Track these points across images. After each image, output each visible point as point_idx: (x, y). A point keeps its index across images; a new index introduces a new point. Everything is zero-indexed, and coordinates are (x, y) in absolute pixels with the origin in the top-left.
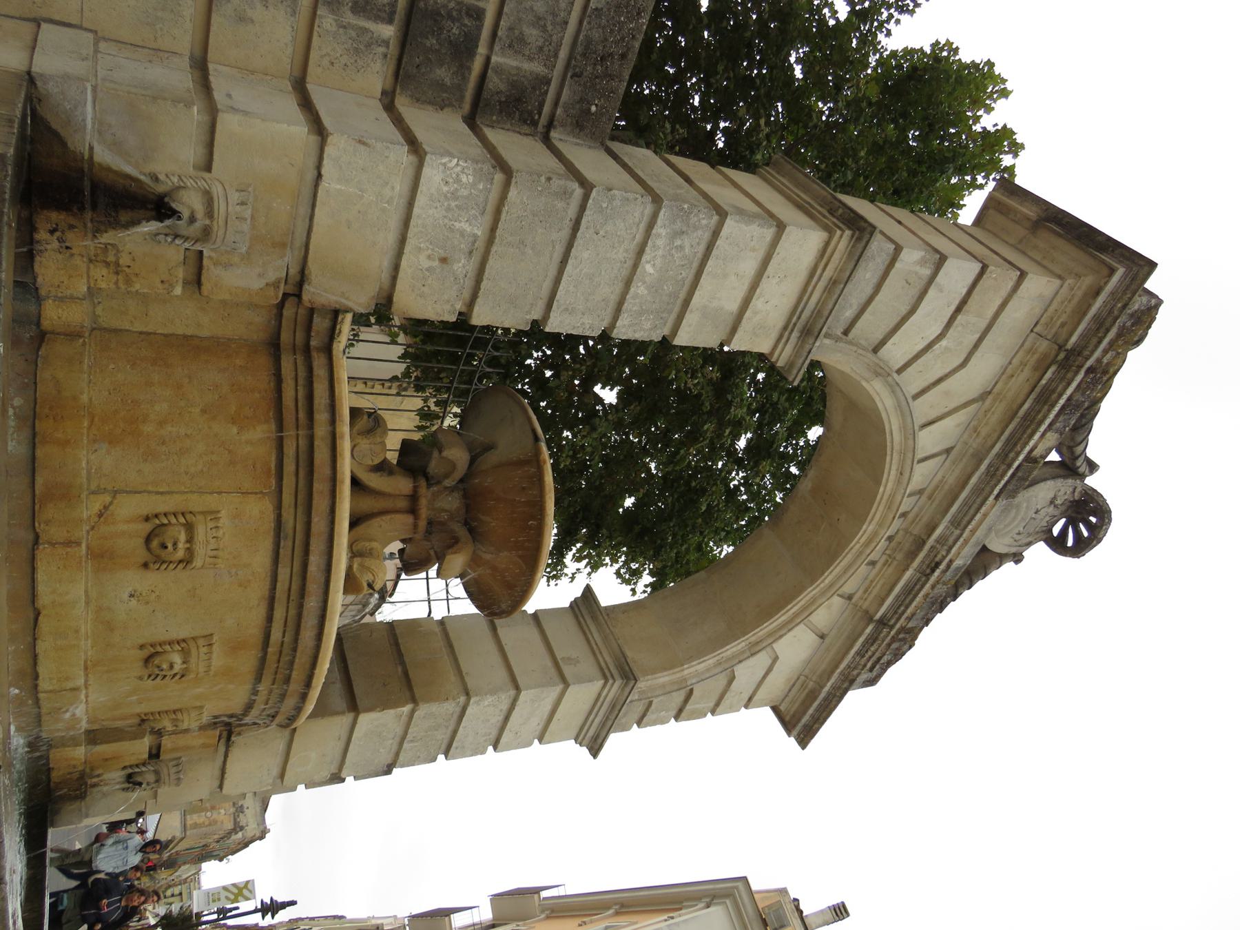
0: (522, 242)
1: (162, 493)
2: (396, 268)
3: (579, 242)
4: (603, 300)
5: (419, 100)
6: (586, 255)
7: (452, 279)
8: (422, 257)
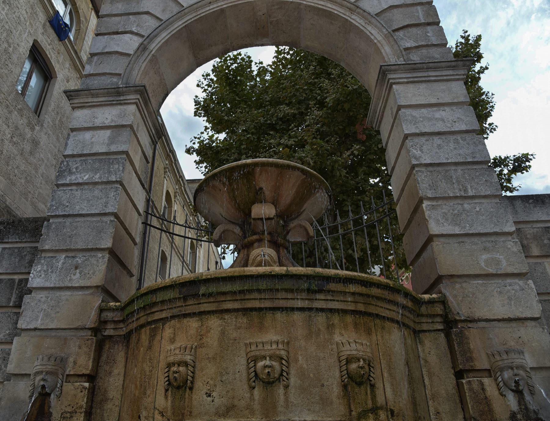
0: (70, 237)
1: (157, 383)
2: (82, 288)
3: (71, 213)
4: (101, 191)
6: (77, 207)
7: (86, 262)
8: (74, 278)
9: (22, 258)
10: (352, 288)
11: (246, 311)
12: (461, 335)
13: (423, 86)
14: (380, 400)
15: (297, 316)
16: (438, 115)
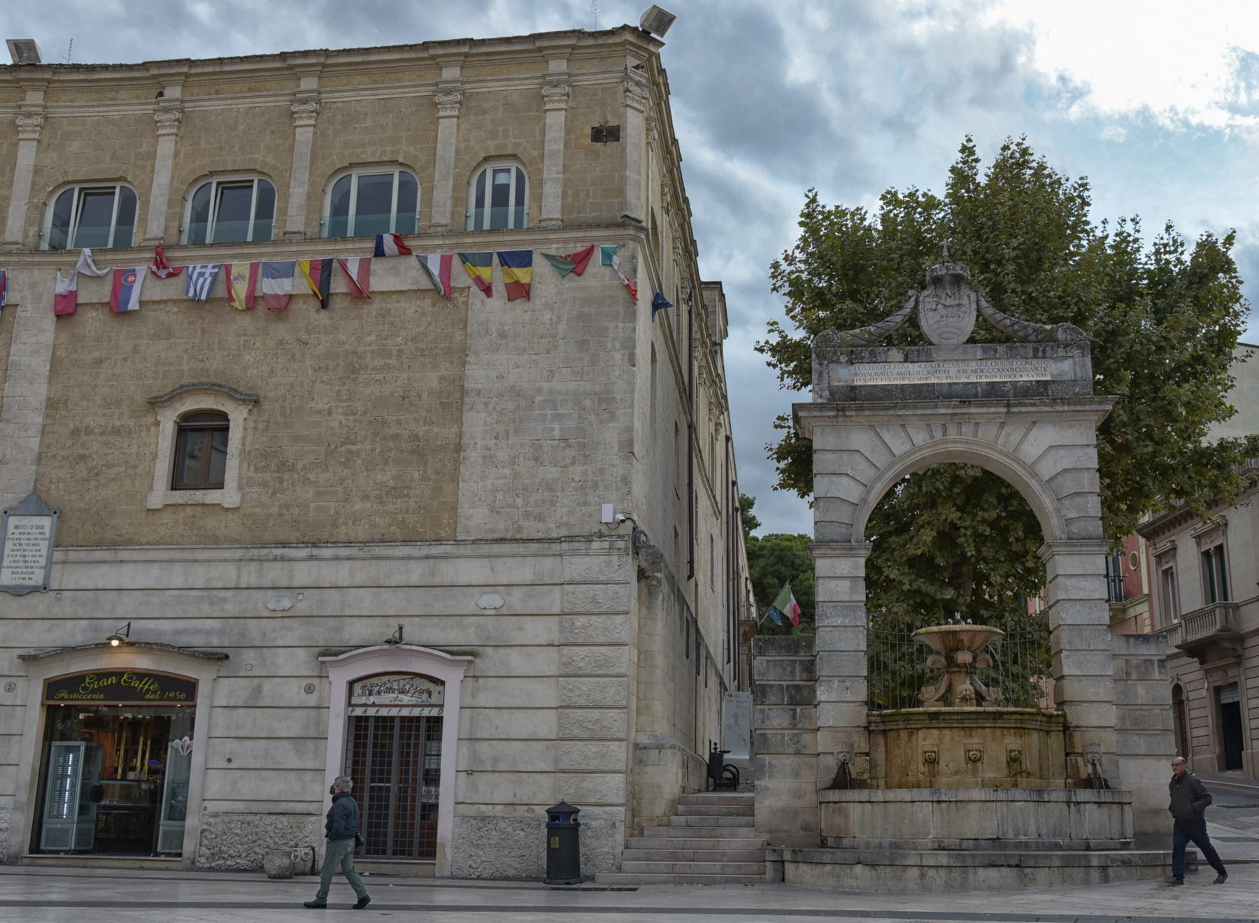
5: (815, 697)
9: (784, 669)
10: (1014, 717)
11: (963, 728)
12: (1071, 736)
13: (1076, 557)
14: (1024, 768)
15: (987, 731)
16: (1082, 585)
